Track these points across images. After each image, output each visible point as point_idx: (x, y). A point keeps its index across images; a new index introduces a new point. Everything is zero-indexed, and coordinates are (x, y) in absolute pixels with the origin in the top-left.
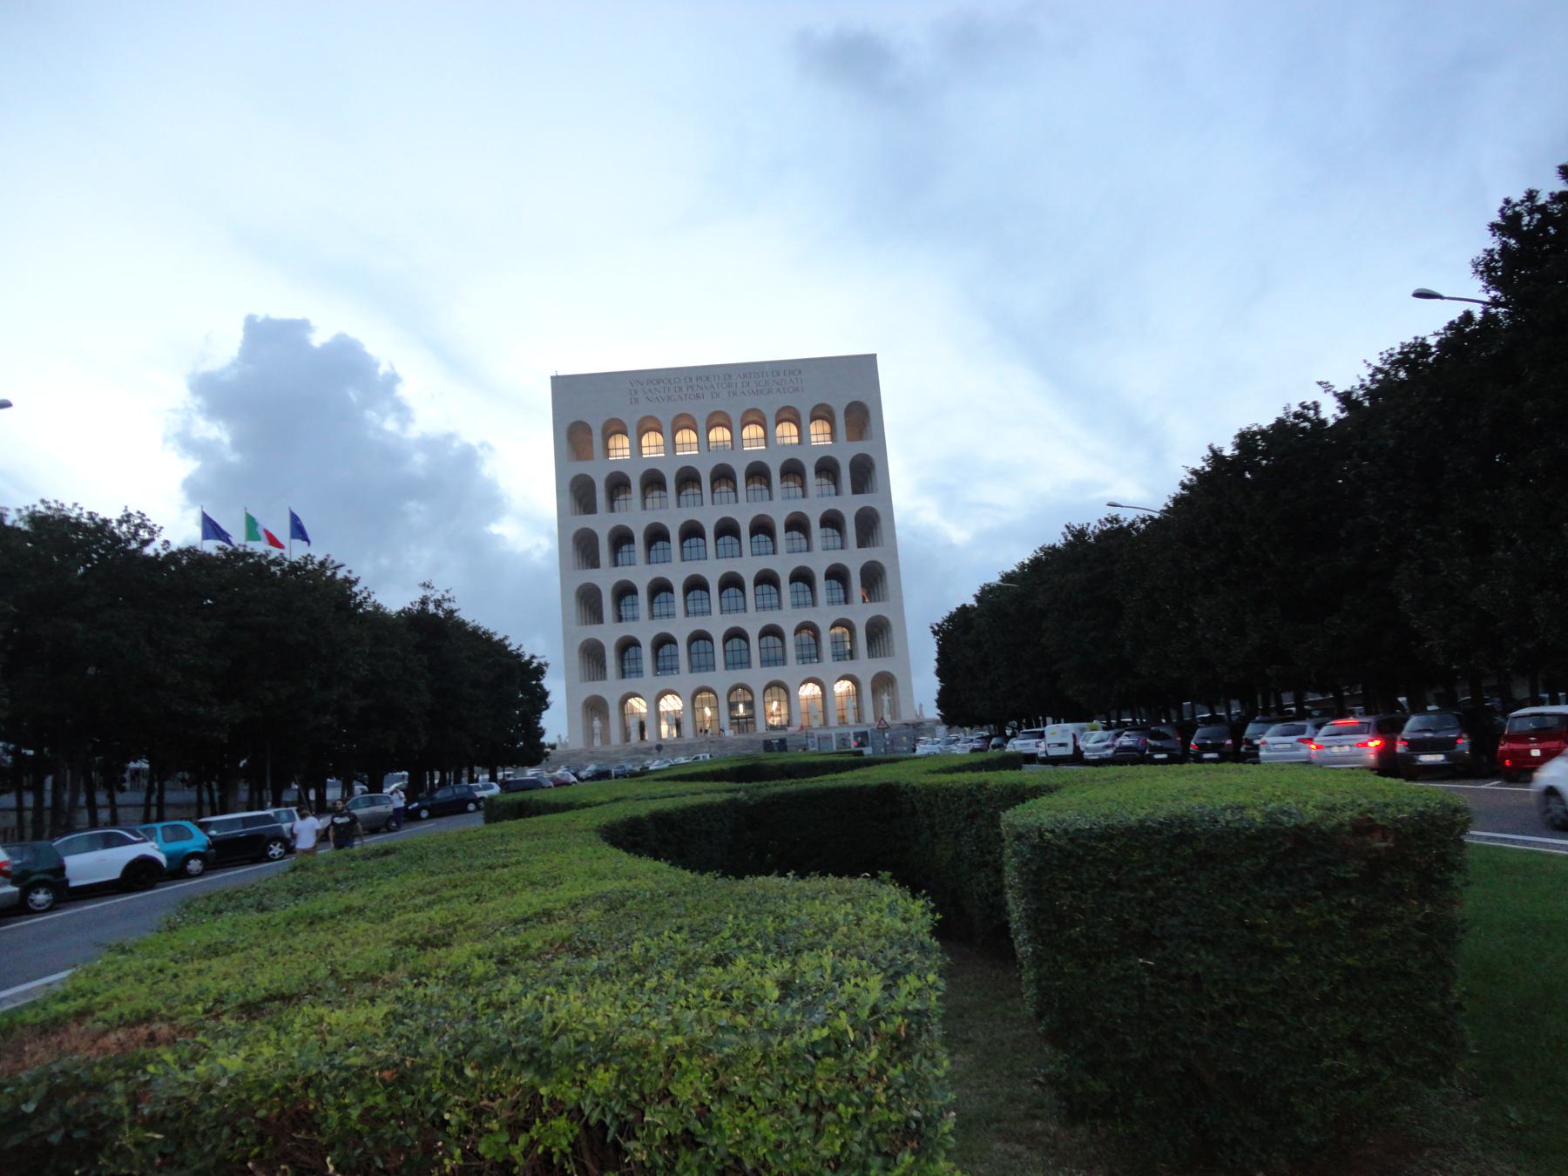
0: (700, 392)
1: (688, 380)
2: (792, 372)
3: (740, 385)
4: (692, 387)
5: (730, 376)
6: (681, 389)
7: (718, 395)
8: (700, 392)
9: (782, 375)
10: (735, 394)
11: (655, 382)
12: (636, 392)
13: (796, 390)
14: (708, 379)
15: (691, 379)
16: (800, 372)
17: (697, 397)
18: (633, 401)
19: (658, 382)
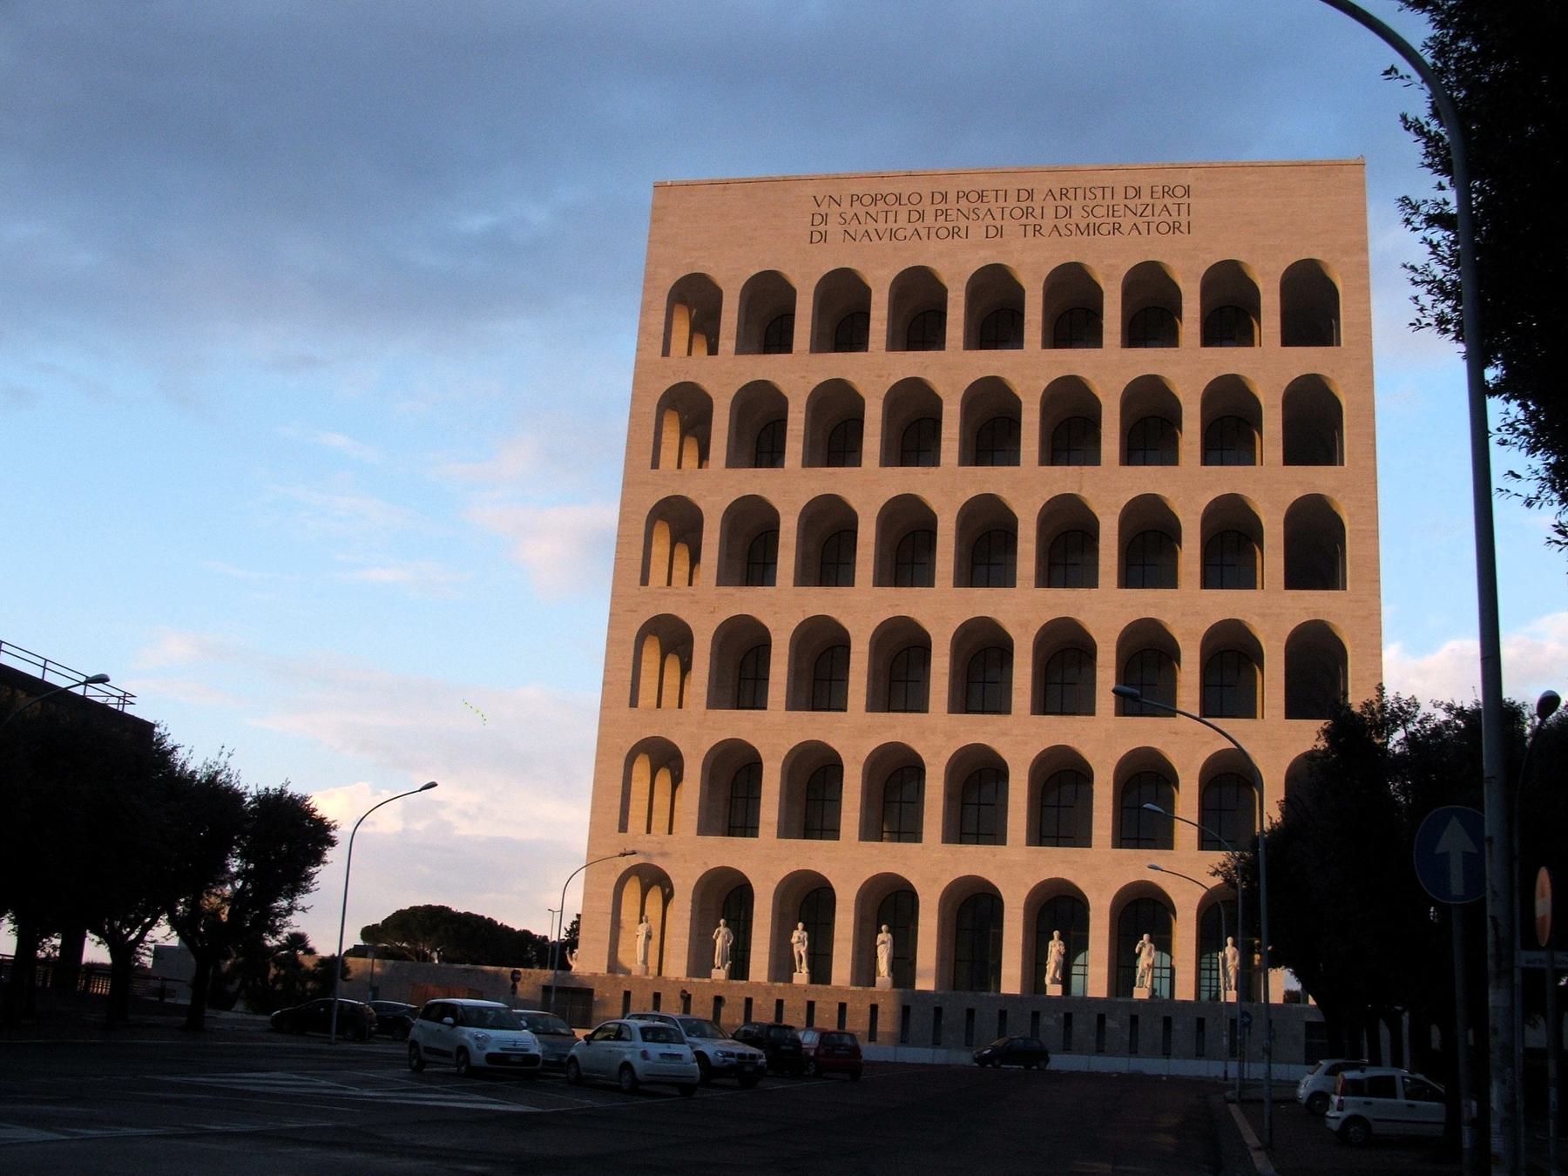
0: (963, 223)
1: (938, 198)
2: (1168, 192)
3: (1050, 212)
4: (945, 213)
5: (1031, 194)
6: (922, 216)
7: (1000, 232)
8: (963, 223)
9: (1146, 199)
10: (1037, 230)
11: (867, 200)
12: (825, 218)
13: (1174, 228)
14: (981, 196)
15: (945, 197)
16: (1187, 192)
17: (953, 233)
18: (817, 237)
19: (875, 200)
